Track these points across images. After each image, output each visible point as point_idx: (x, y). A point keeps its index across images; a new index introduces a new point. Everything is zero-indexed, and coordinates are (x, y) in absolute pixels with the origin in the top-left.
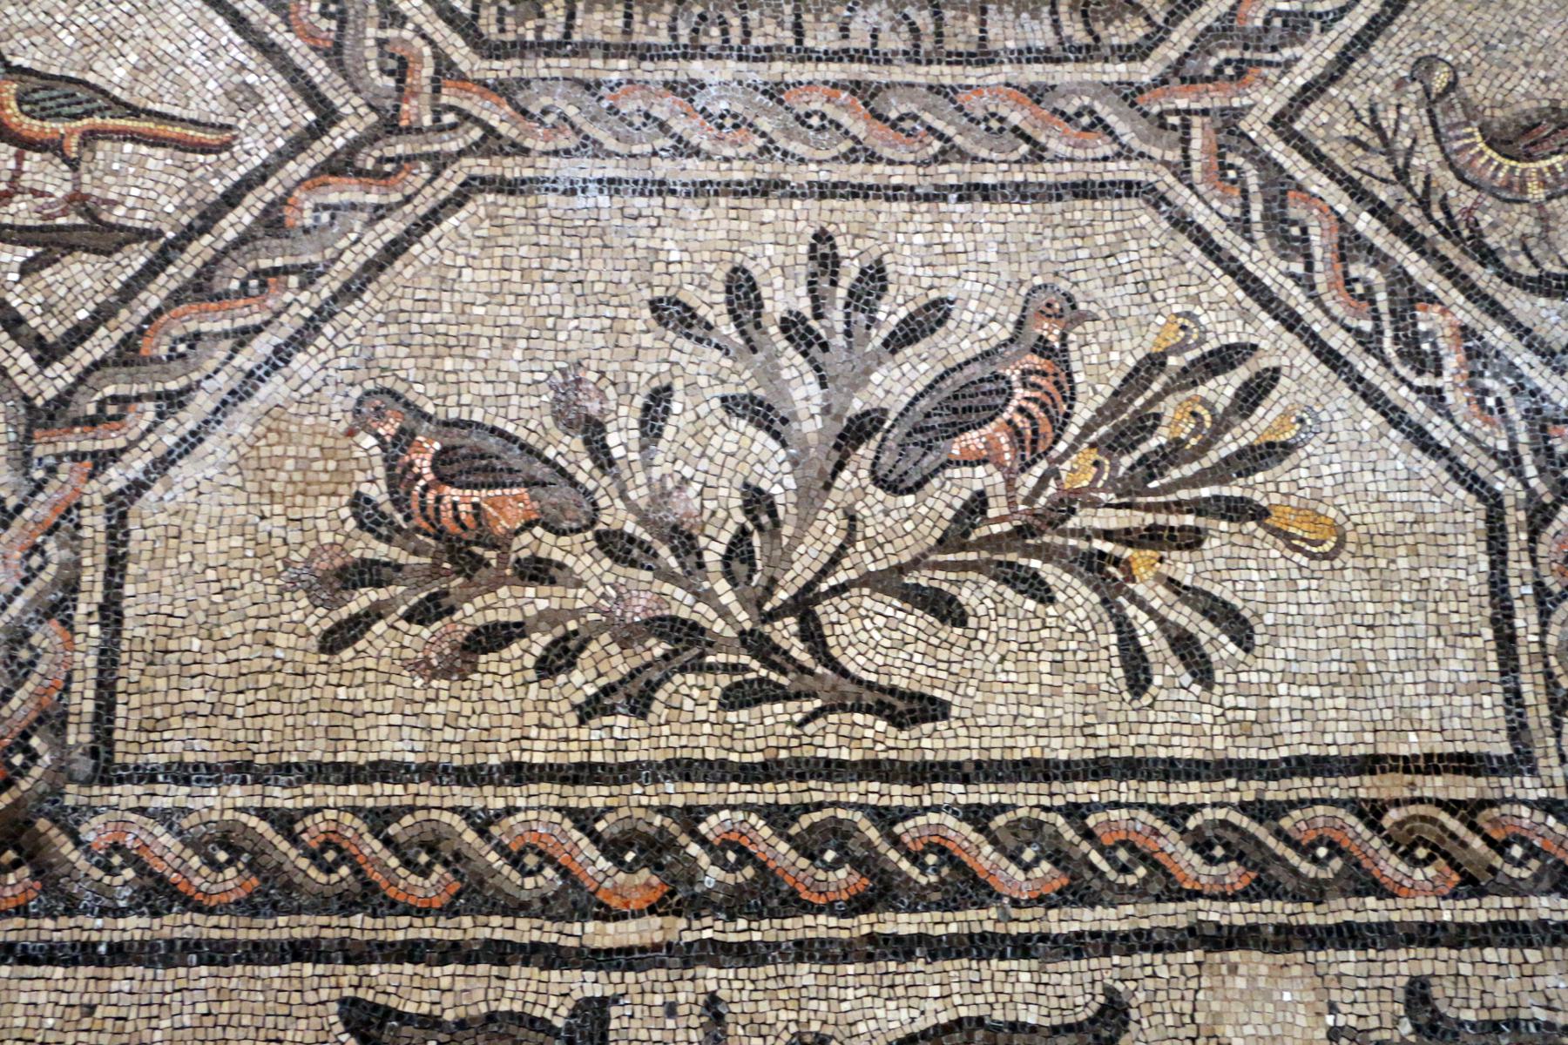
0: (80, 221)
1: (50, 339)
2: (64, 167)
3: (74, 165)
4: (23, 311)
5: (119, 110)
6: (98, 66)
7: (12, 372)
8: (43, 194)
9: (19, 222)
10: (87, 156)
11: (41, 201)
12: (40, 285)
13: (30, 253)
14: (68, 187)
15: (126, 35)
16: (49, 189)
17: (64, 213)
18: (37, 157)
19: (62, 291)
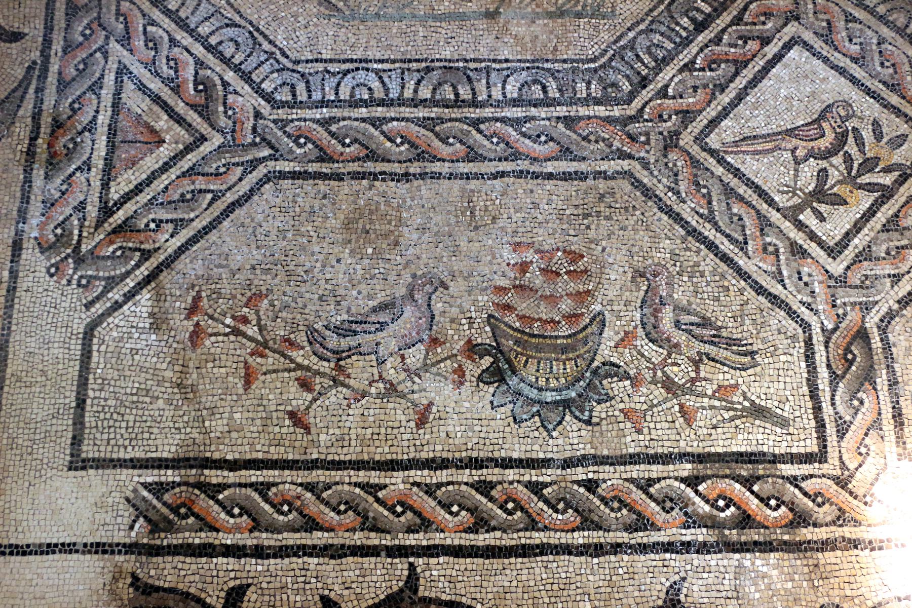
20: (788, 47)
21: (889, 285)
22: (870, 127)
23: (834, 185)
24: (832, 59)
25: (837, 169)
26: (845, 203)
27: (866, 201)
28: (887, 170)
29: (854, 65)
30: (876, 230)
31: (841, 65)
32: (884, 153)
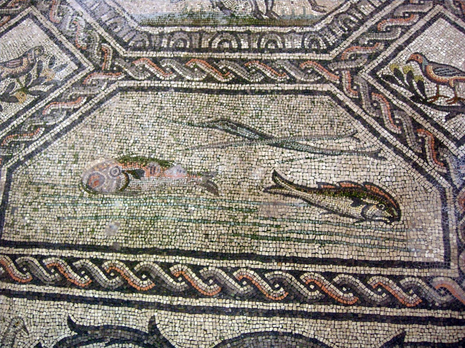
0: (459, 105)
1: (459, 139)
2: (451, 90)
3: (454, 89)
4: (449, 130)
5: (462, 74)
6: (454, 62)
7: (450, 148)
8: (447, 97)
9: (441, 105)
10: (457, 87)
11: (447, 99)
12: (452, 123)
13: (447, 114)
14: (453, 95)
15: (460, 53)
16: (448, 96)
17: (454, 102)
18: (443, 87)
19: (459, 125)
20: (22, 20)
21: (23, 147)
22: (49, 60)
23: (14, 92)
24: (44, 24)
25: (20, 83)
26: (18, 101)
27: (29, 99)
28: (47, 84)
29: (54, 27)
30: (27, 116)
31: (48, 27)
32: (50, 74)
